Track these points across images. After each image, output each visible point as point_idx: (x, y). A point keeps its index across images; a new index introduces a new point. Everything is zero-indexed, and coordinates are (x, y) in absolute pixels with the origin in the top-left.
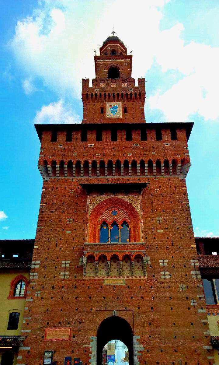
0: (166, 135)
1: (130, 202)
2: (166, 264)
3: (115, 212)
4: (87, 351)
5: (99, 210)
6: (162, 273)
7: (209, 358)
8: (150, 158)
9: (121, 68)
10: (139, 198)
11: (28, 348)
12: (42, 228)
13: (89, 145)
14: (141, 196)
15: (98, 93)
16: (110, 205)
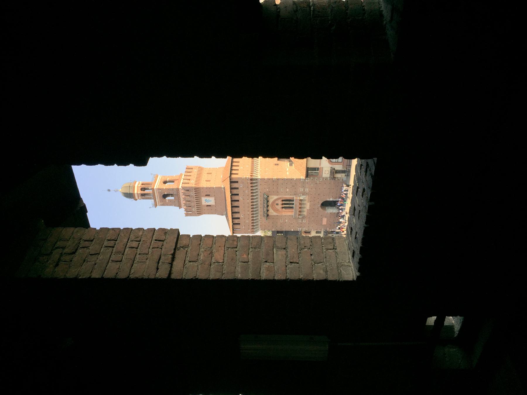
0: (235, 185)
1: (273, 200)
2: (302, 189)
3: (277, 204)
4: (331, 213)
5: (276, 210)
6: (306, 191)
7: (337, 180)
8: (250, 193)
9: (164, 194)
10: (270, 197)
11: (328, 229)
12: (284, 229)
13: (242, 216)
14: (269, 196)
15: (197, 209)
16: (274, 206)
